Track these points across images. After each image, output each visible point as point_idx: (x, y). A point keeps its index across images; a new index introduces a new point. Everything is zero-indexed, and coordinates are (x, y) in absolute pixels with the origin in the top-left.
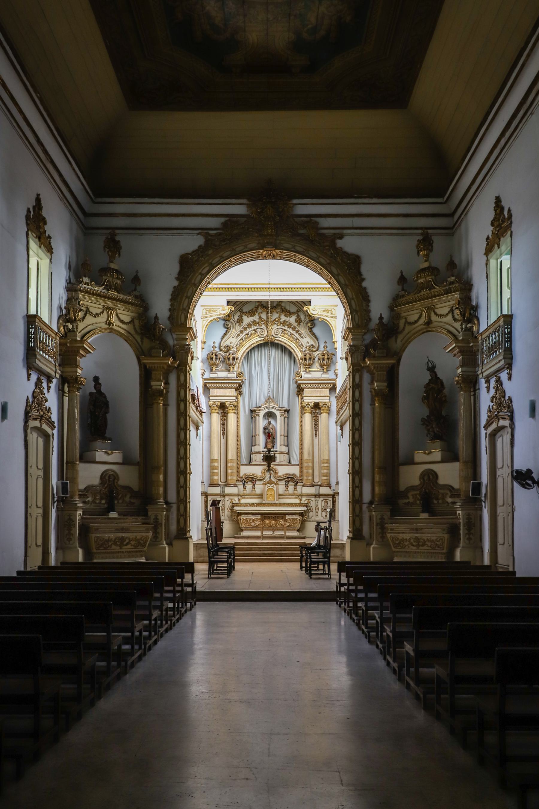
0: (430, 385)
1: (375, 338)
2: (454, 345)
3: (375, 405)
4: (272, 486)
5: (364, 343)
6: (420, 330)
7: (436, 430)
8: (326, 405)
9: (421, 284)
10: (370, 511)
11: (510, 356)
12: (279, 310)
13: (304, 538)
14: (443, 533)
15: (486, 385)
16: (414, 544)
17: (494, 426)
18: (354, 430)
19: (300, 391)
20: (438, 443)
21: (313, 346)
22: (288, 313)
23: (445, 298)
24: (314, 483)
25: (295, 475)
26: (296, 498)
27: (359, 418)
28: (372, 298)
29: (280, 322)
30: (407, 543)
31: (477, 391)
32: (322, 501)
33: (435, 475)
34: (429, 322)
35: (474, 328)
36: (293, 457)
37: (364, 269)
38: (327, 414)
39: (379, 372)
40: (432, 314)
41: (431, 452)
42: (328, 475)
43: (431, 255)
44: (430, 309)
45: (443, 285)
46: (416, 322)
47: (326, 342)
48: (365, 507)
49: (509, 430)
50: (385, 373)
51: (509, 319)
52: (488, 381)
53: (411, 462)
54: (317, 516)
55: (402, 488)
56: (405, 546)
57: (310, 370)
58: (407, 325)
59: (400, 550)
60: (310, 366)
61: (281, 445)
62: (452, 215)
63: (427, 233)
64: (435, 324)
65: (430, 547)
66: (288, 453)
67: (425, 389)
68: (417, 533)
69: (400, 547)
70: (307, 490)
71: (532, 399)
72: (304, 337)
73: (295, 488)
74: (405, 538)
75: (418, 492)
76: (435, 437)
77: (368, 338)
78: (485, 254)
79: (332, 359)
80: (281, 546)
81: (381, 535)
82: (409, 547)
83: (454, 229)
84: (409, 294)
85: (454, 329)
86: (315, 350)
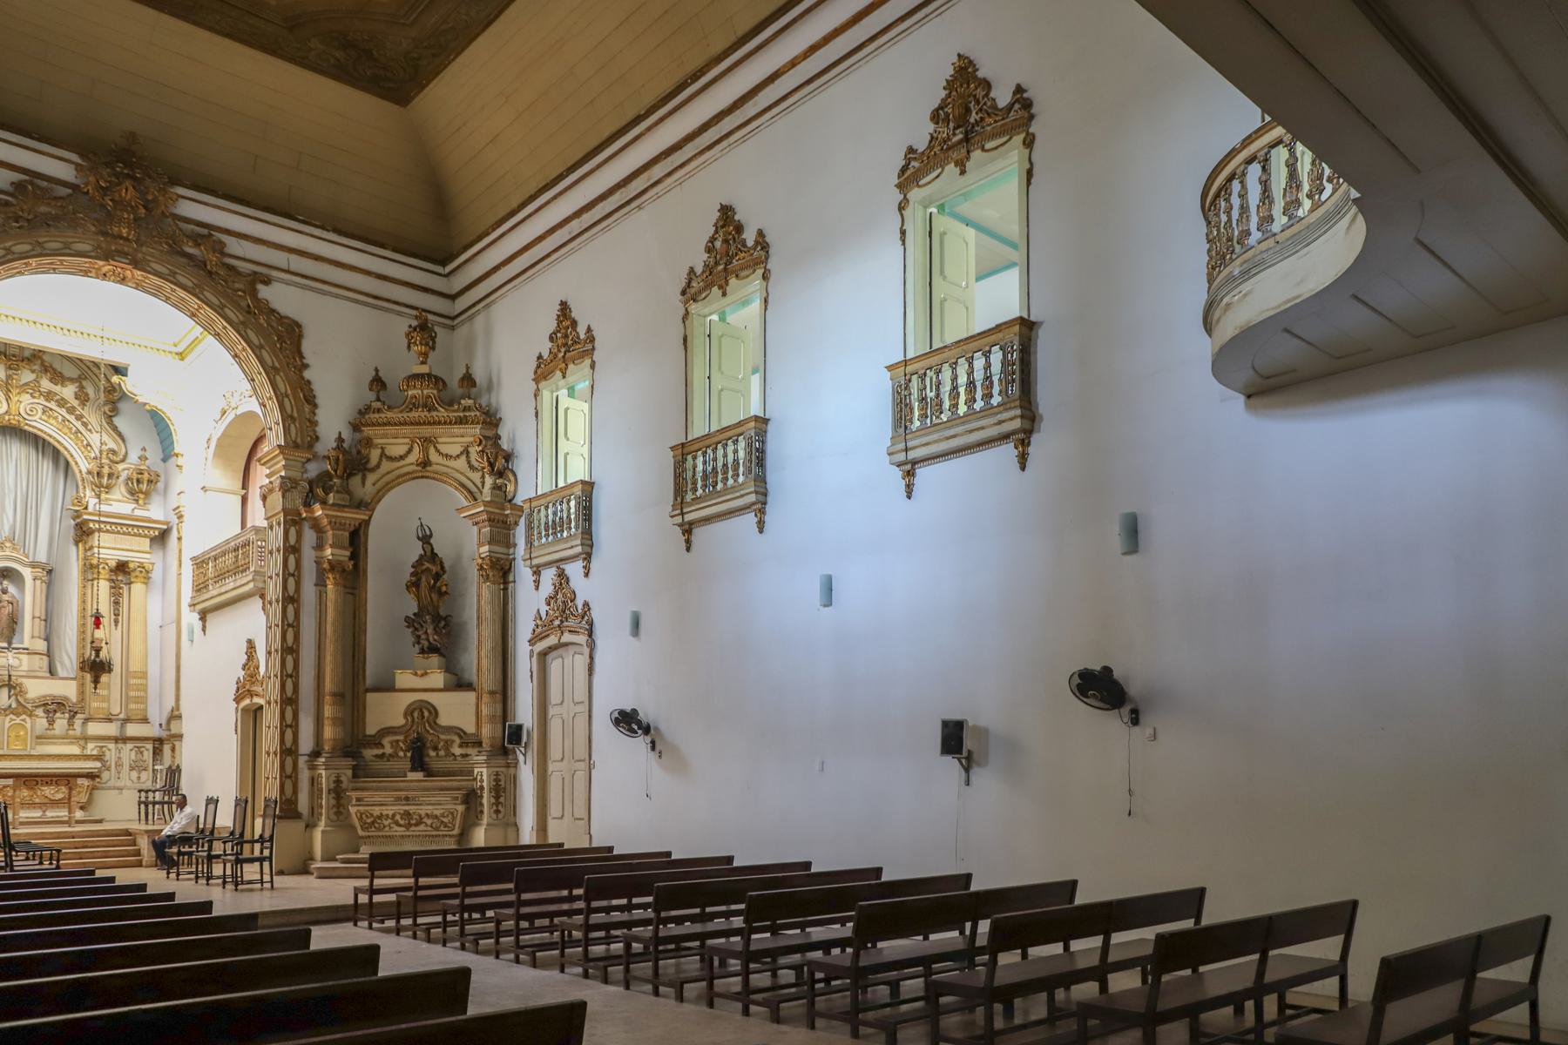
0: (423, 565)
1: (328, 471)
2: (482, 509)
3: (326, 586)
4: (23, 720)
5: (305, 476)
6: (408, 473)
7: (433, 638)
8: (143, 568)
9: (412, 398)
10: (312, 768)
11: (590, 542)
12: (36, 367)
13: (100, 821)
14: (455, 804)
15: (534, 578)
16: (402, 822)
17: (552, 640)
18: (286, 627)
19: (83, 532)
20: (435, 659)
21: (114, 452)
22: (58, 378)
23: (456, 429)
24: (111, 717)
25: (66, 698)
26: (72, 743)
27: (295, 605)
28: (318, 401)
29: (40, 391)
30: (386, 823)
31: (511, 585)
32: (131, 750)
33: (434, 712)
34: (425, 463)
35: (508, 487)
36: (62, 663)
37: (307, 347)
38: (143, 586)
39: (337, 532)
40: (432, 450)
41: (426, 674)
42: (143, 700)
43: (432, 354)
44: (428, 441)
45: (452, 408)
46: (402, 458)
47: (144, 449)
48: (302, 761)
49: (586, 651)
50: (347, 534)
51: (588, 488)
52: (537, 572)
53: (388, 687)
54: (119, 778)
55: (371, 730)
56: (384, 827)
57: (107, 496)
58: (384, 460)
59: (376, 834)
60: (109, 488)
61: (33, 637)
62: (452, 298)
63: (426, 320)
64: (434, 467)
65: (431, 827)
66: (49, 654)
67: (413, 570)
68: (409, 805)
69: (373, 829)
70: (94, 729)
71: (635, 609)
72: (93, 431)
73: (71, 723)
74: (384, 813)
75: (401, 738)
76: (433, 649)
77: (313, 470)
78: (534, 380)
79: (156, 483)
80: (73, 838)
81: (335, 810)
82: (390, 828)
83: (456, 322)
84: (390, 408)
85: (469, 482)
86: (118, 459)
